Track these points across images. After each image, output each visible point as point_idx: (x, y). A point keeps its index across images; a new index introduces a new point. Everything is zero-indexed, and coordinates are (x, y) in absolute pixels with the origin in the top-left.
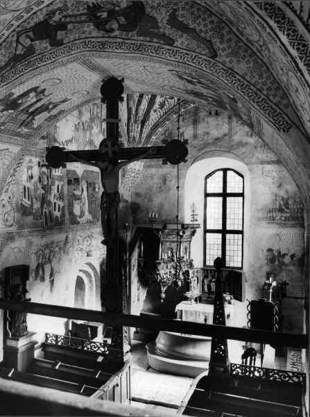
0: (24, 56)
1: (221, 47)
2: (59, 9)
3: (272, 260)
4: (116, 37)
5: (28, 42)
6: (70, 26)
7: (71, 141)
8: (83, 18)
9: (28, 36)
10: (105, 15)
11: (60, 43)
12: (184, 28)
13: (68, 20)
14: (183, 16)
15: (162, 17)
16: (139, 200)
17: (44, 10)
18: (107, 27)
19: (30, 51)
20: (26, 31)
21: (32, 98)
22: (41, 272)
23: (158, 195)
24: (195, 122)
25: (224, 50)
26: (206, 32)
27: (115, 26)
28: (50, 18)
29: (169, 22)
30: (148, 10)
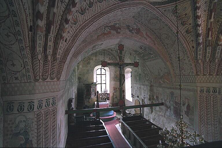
3: (115, 90)
8: (126, 28)
12: (149, 37)
13: (121, 27)
14: (148, 34)
15: (144, 33)
16: (80, 76)
19: (110, 33)
23: (86, 75)
24: (96, 56)
29: (146, 35)
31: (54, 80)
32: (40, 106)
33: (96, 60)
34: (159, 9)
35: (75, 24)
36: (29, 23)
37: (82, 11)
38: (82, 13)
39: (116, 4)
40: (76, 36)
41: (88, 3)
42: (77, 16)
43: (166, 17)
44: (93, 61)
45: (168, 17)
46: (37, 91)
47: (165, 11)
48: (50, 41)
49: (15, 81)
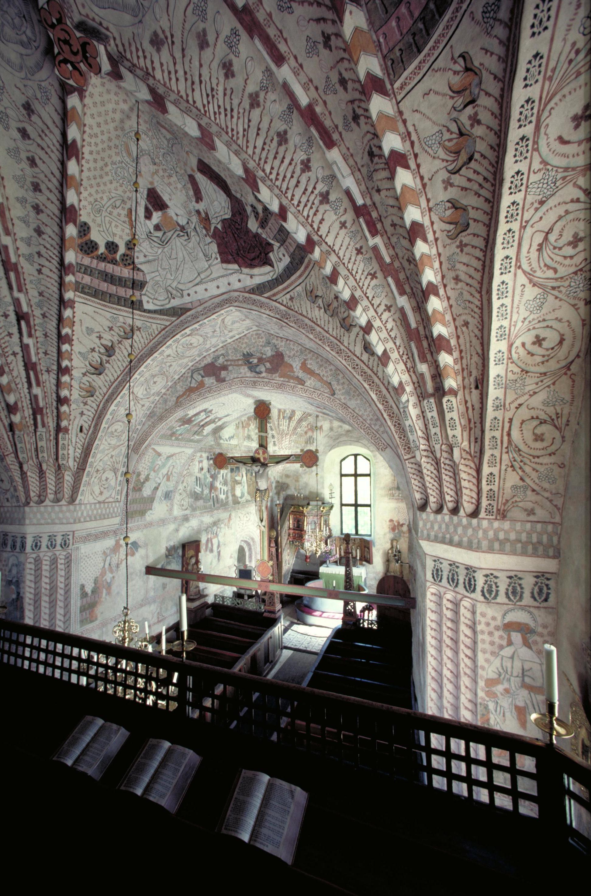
0: (197, 388)
1: (338, 388)
2: (223, 355)
4: (263, 378)
5: (200, 378)
6: (230, 368)
7: (233, 437)
8: (240, 362)
9: (200, 374)
10: (255, 361)
11: (223, 380)
12: (311, 373)
14: (311, 364)
15: (296, 365)
17: (212, 356)
18: (257, 370)
19: (201, 385)
20: (198, 370)
21: (203, 416)
22: (210, 545)
25: (340, 390)
26: (327, 377)
27: (263, 369)
28: (216, 361)
29: (301, 368)
30: (286, 359)
31: (60, 503)
32: (36, 546)
33: (331, 429)
34: (275, 301)
35: (92, 396)
36: (5, 421)
37: (96, 369)
38: (97, 372)
39: (167, 327)
40: (99, 417)
41: (103, 350)
42: (91, 380)
43: (301, 317)
44: (323, 434)
45: (305, 313)
46: (27, 522)
47: (291, 299)
48: (41, 440)
49: (8, 504)
